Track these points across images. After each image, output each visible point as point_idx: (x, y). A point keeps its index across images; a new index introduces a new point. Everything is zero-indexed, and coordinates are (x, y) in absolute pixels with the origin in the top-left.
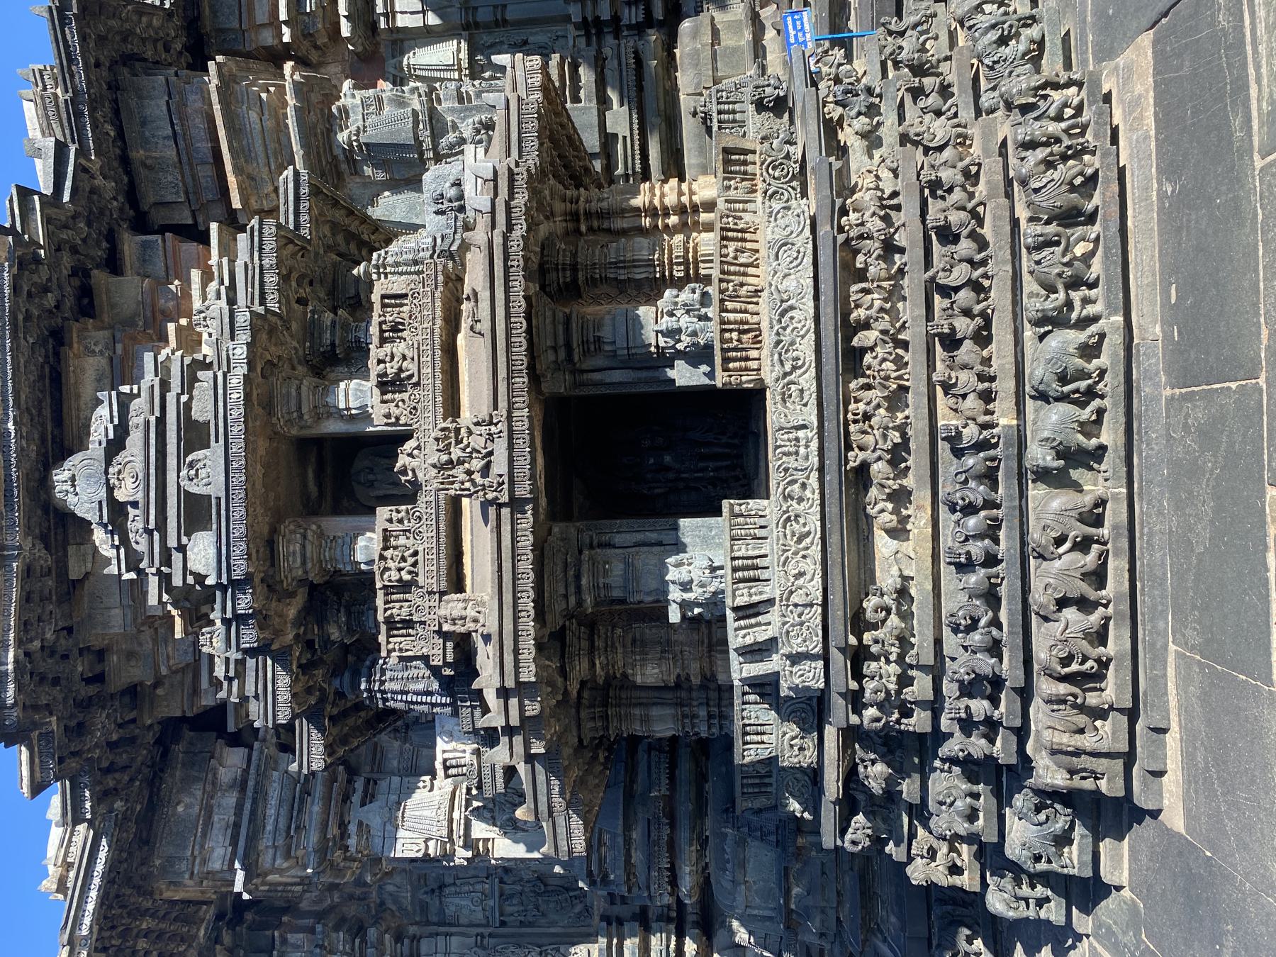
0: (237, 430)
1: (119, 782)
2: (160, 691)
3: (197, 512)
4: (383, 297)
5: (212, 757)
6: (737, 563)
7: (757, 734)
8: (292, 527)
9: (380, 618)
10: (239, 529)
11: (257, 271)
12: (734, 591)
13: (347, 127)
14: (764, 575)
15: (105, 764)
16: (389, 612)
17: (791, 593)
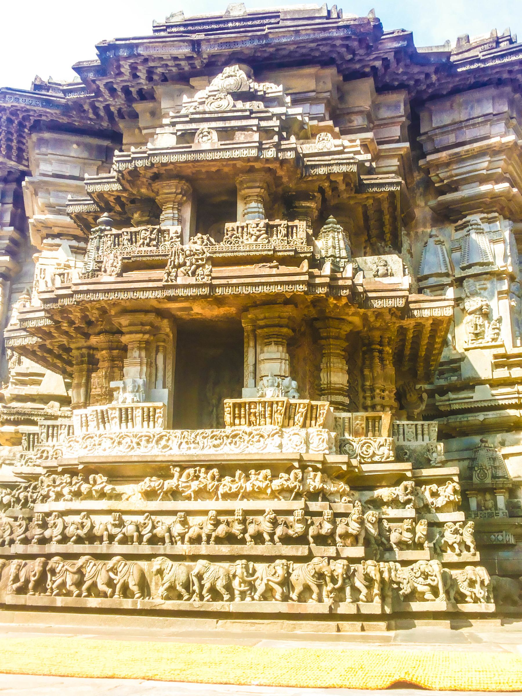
0: (227, 155)
1: (88, 112)
2: (137, 131)
3: (187, 137)
4: (296, 226)
5: (103, 162)
6: (130, 410)
7: (53, 433)
8: (185, 187)
9: (124, 230)
10: (174, 159)
11: (327, 163)
12: (114, 409)
13: (482, 222)
14: (124, 425)
15: (97, 104)
16: (125, 233)
17: (112, 439)
